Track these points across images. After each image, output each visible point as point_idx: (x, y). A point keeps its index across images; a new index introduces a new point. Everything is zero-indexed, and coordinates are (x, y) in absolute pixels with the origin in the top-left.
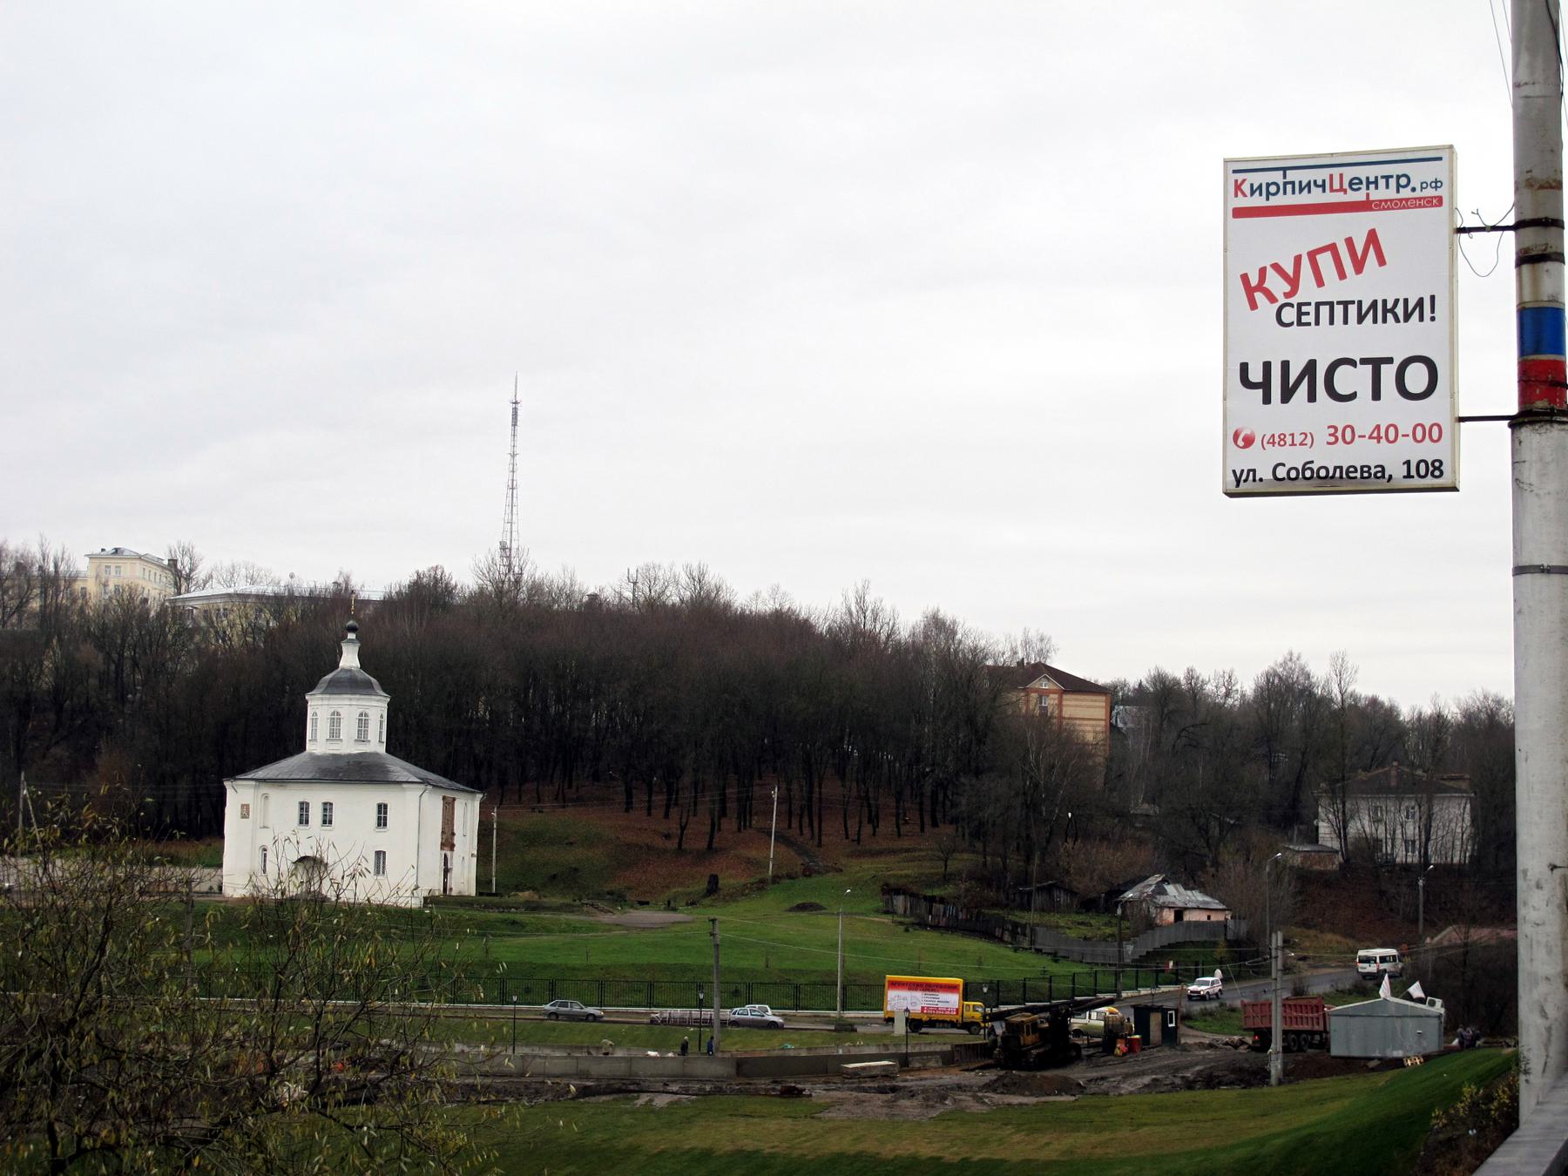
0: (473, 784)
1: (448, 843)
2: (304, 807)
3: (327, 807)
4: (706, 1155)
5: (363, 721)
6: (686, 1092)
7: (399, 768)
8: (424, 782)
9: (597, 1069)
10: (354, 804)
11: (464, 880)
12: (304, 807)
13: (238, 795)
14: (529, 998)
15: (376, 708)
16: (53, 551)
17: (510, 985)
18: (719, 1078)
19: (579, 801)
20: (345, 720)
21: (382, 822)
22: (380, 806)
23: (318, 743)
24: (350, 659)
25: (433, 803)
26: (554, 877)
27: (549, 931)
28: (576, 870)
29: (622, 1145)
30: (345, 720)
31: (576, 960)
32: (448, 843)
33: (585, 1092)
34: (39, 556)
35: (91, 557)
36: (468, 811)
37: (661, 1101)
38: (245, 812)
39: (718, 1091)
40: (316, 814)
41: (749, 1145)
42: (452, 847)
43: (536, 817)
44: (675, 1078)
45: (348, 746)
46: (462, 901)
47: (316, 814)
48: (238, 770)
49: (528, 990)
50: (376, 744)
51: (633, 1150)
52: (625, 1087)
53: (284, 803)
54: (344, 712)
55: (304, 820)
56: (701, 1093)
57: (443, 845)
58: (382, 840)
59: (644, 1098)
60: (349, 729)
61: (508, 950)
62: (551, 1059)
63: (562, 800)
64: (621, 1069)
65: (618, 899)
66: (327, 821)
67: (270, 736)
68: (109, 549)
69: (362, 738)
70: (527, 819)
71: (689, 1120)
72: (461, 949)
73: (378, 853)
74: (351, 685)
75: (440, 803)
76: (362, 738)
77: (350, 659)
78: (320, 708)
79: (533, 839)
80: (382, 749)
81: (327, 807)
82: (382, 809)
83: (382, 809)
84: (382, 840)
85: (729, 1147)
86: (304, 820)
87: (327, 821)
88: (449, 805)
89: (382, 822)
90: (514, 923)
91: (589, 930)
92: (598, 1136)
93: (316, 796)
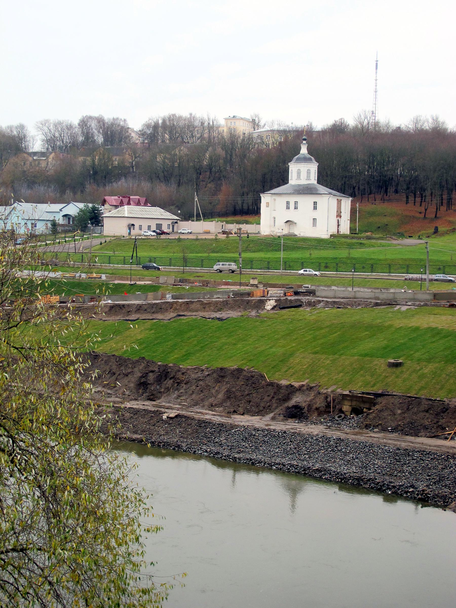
1: (339, 215)
2: (288, 203)
3: (296, 203)
4: (417, 329)
5: (309, 172)
6: (414, 305)
7: (322, 189)
8: (330, 194)
9: (382, 296)
10: (306, 202)
11: (345, 228)
12: (288, 203)
13: (265, 199)
14: (364, 270)
15: (313, 167)
16: (212, 117)
17: (357, 266)
18: (428, 300)
19: (389, 200)
20: (302, 172)
21: (315, 208)
22: (314, 202)
23: (293, 180)
24: (304, 150)
25: (333, 201)
26: (379, 227)
27: (373, 246)
28: (387, 225)
29: (386, 324)
30: (302, 172)
31: (382, 257)
32: (339, 215)
33: (377, 304)
34: (207, 119)
35: (226, 119)
36: (347, 203)
37: (404, 308)
38: (268, 205)
39: (426, 305)
40: (292, 206)
41: (434, 325)
42: (341, 217)
43: (374, 206)
44: (411, 300)
45: (303, 181)
46: (345, 236)
47: (292, 206)
48: (264, 191)
49: (363, 267)
50: (313, 180)
51: (390, 326)
52: (391, 303)
53: (281, 202)
54: (302, 169)
55: (288, 208)
56: (419, 306)
57: (337, 216)
58: (315, 214)
59: (398, 307)
60: (304, 175)
61: (357, 253)
62: (364, 292)
63: (383, 200)
64: (391, 296)
65: (401, 235)
66: (296, 208)
67: (275, 177)
68: (232, 116)
69: (308, 178)
70: (369, 207)
71: (413, 316)
72: (343, 253)
73: (314, 219)
74: (305, 160)
75: (336, 201)
76: (308, 178)
77: (304, 150)
78: (293, 168)
79: (372, 214)
80: (316, 182)
81: (296, 203)
82: (315, 203)
83: (315, 203)
85: (426, 326)
86: (288, 208)
87: (296, 208)
88: (339, 202)
89: (315, 208)
90: (361, 244)
91: (388, 246)
92: (379, 321)
93: (292, 199)
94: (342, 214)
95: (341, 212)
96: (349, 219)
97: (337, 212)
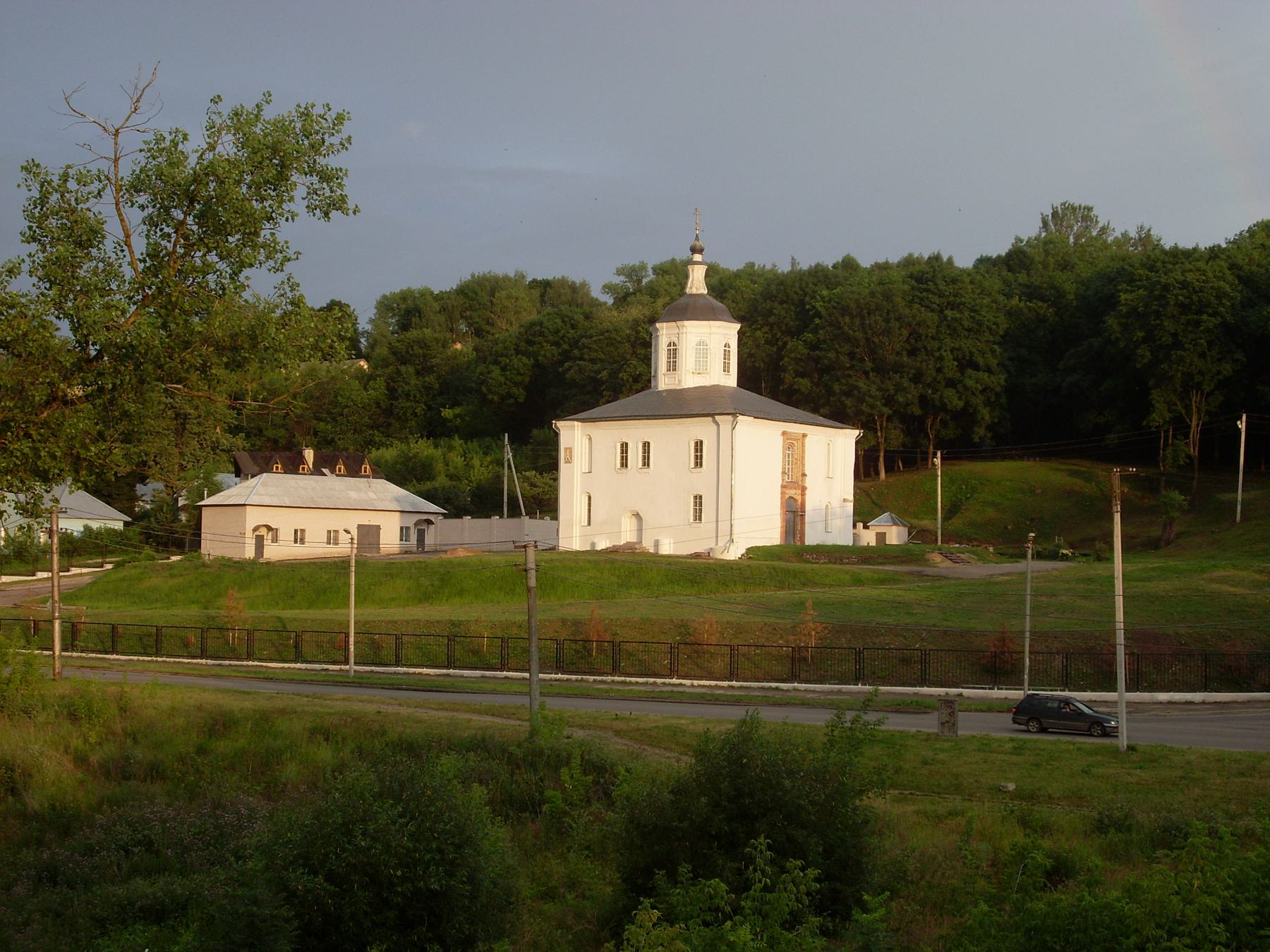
0: (835, 413)
2: (624, 447)
3: (646, 445)
12: (624, 447)
40: (635, 455)
47: (635, 455)
55: (624, 464)
58: (701, 482)
60: (687, 359)
66: (646, 462)
75: (779, 441)
81: (646, 445)
82: (699, 446)
84: (701, 482)
86: (624, 464)
87: (646, 462)
94: (808, 482)
95: (804, 475)
96: (851, 498)
97: (784, 473)
